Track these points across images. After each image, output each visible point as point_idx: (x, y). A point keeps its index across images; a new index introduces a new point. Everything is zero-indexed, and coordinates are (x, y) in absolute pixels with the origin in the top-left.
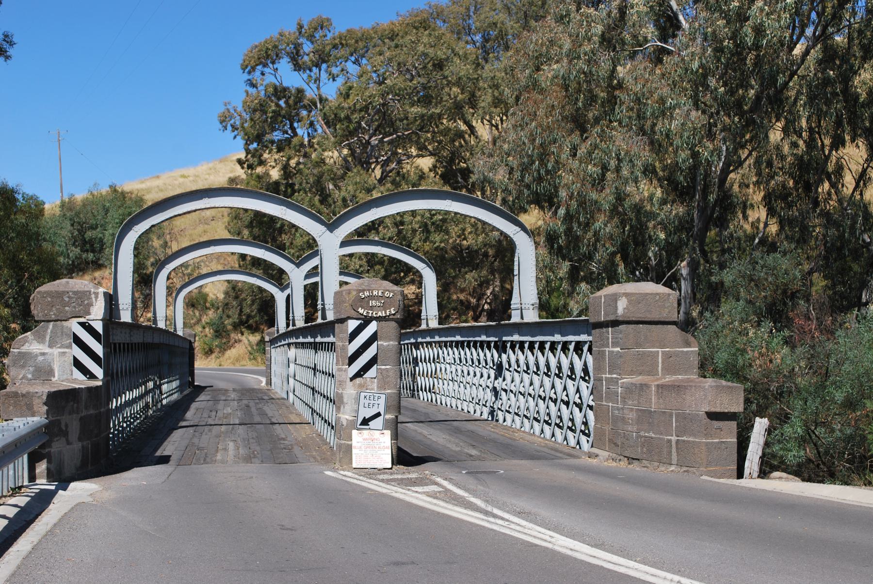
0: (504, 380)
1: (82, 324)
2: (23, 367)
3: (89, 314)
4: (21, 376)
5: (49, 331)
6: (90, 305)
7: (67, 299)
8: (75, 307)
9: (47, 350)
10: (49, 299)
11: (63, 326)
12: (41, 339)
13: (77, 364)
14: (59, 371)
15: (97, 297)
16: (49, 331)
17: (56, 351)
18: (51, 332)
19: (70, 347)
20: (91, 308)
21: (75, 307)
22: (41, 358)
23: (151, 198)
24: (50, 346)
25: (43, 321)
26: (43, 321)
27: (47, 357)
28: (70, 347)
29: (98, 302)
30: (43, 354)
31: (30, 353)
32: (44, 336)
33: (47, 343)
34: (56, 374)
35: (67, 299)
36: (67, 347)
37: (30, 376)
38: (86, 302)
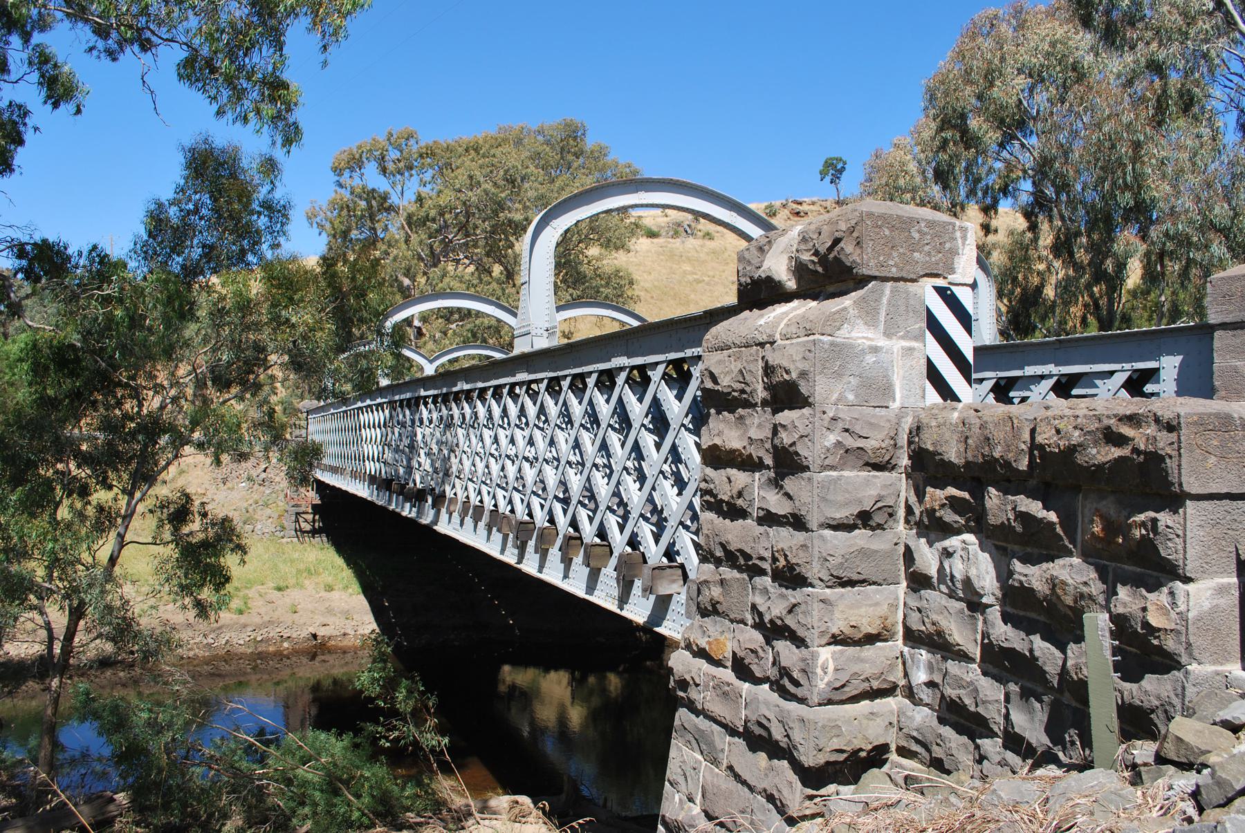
0: (1171, 457)
1: (941, 291)
2: (838, 375)
3: (952, 270)
4: (835, 396)
5: (885, 300)
6: (954, 252)
7: (916, 236)
8: (929, 254)
9: (882, 342)
10: (887, 232)
11: (908, 293)
12: (869, 313)
13: (934, 375)
14: (902, 388)
15: (964, 238)
16: (885, 300)
17: (897, 345)
18: (889, 303)
19: (921, 338)
20: (956, 259)
21: (929, 254)
22: (870, 359)
23: (647, 174)
24: (888, 334)
25: (875, 278)
26: (875, 278)
27: (882, 356)
28: (921, 338)
29: (967, 248)
30: (875, 350)
31: (852, 346)
32: (876, 311)
33: (882, 327)
34: (898, 396)
35: (916, 236)
36: (916, 338)
37: (851, 397)
38: (948, 246)
